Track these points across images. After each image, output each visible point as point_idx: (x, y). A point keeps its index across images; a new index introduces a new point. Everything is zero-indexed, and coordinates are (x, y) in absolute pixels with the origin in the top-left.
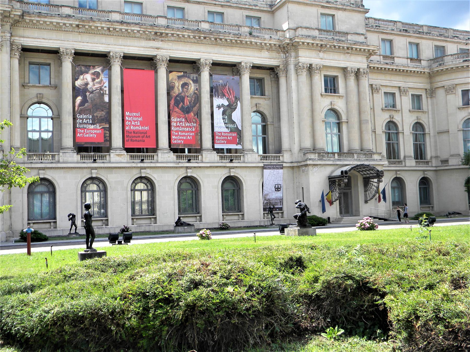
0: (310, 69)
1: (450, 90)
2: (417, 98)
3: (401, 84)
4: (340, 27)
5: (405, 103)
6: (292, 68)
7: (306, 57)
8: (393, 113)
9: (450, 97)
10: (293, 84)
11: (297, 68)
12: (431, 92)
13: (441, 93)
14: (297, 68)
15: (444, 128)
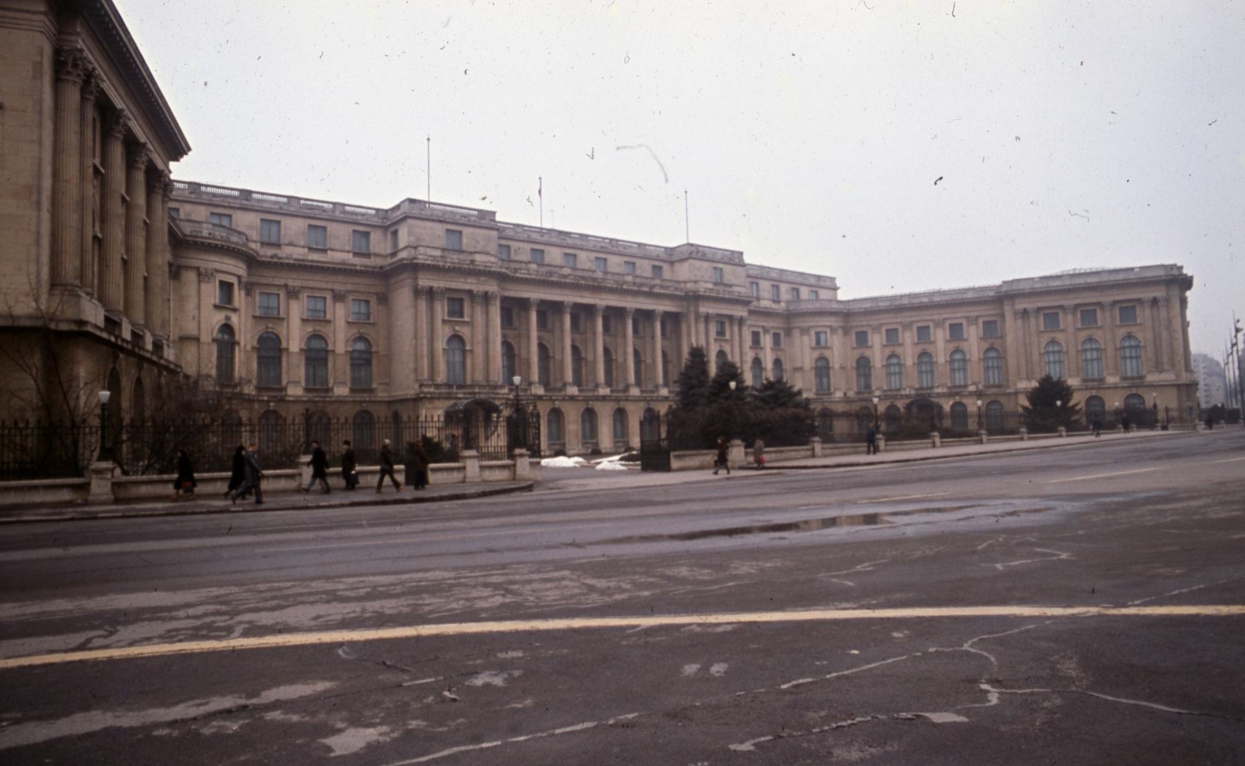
0: (707, 318)
1: (805, 331)
2: (776, 337)
3: (765, 324)
4: (726, 280)
5: (767, 341)
6: (692, 316)
7: (705, 309)
8: (759, 351)
9: (806, 339)
10: (693, 329)
11: (697, 316)
12: (788, 332)
13: (796, 333)
14: (697, 316)
15: (798, 365)
